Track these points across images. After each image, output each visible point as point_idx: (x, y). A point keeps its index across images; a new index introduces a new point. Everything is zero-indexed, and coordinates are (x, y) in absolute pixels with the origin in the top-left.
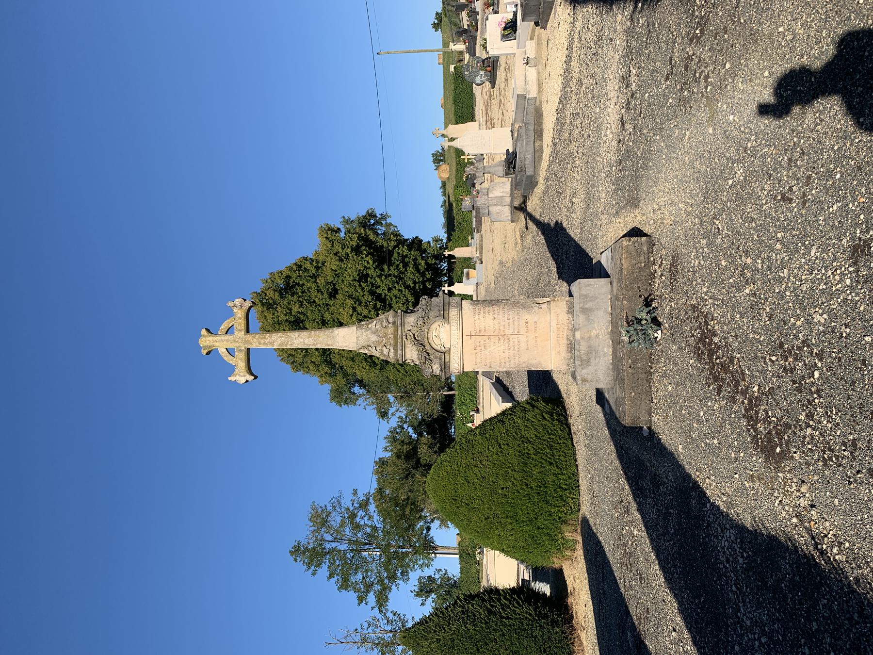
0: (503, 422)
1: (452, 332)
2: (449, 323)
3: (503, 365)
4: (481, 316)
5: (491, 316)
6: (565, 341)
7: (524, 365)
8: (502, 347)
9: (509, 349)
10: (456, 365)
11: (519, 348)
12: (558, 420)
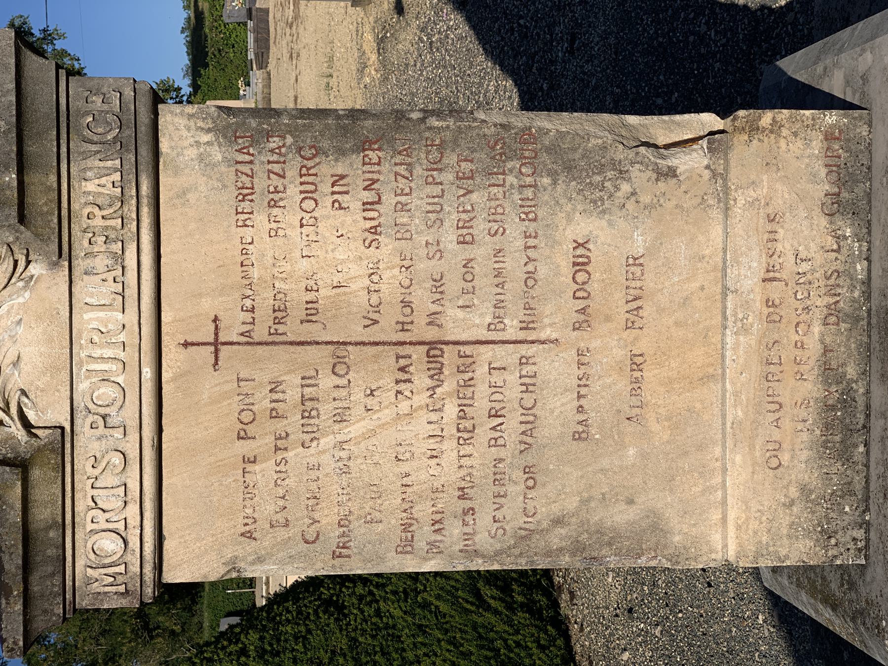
0: (340, 608)
1: (88, 320)
2: (64, 254)
3: (424, 534)
4: (290, 217)
5: (354, 220)
6: (810, 388)
7: (557, 538)
8: (421, 426)
9: (465, 433)
10: (110, 545)
11: (529, 427)
12: (529, 607)
